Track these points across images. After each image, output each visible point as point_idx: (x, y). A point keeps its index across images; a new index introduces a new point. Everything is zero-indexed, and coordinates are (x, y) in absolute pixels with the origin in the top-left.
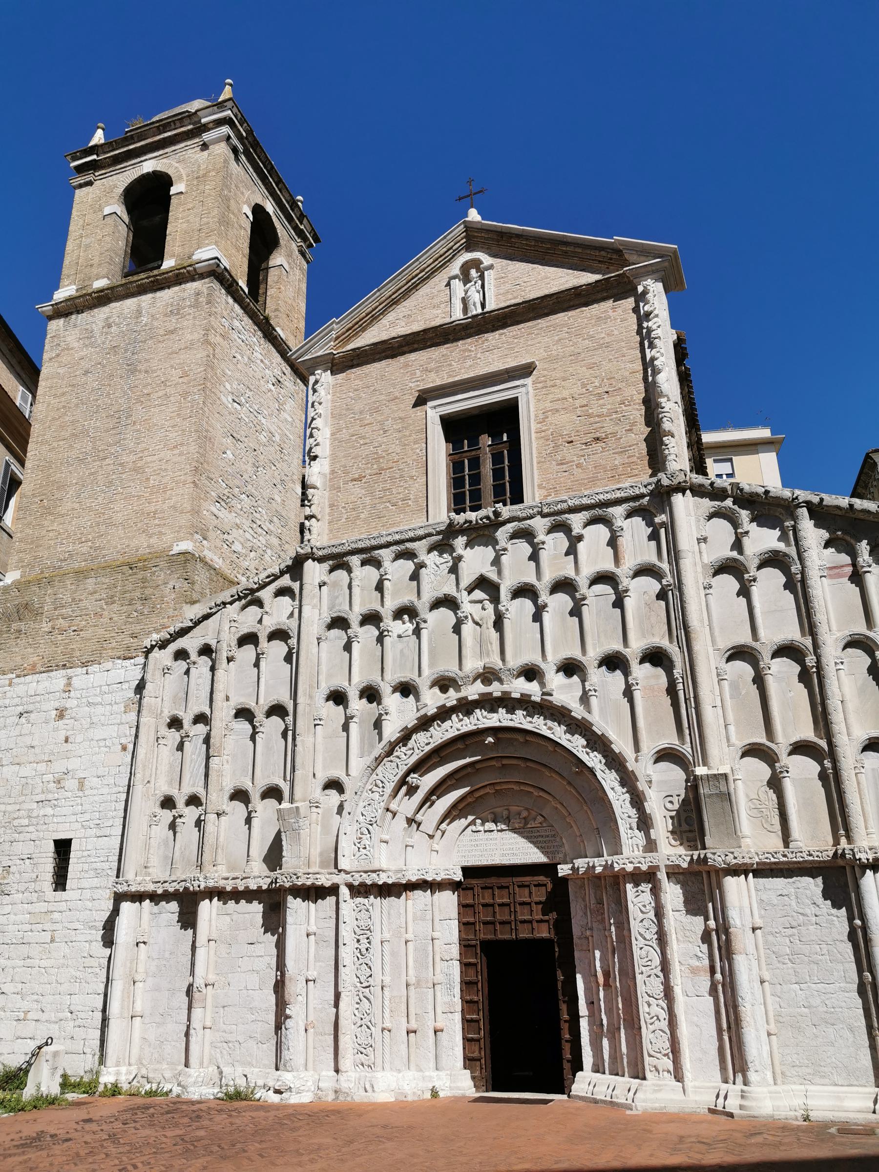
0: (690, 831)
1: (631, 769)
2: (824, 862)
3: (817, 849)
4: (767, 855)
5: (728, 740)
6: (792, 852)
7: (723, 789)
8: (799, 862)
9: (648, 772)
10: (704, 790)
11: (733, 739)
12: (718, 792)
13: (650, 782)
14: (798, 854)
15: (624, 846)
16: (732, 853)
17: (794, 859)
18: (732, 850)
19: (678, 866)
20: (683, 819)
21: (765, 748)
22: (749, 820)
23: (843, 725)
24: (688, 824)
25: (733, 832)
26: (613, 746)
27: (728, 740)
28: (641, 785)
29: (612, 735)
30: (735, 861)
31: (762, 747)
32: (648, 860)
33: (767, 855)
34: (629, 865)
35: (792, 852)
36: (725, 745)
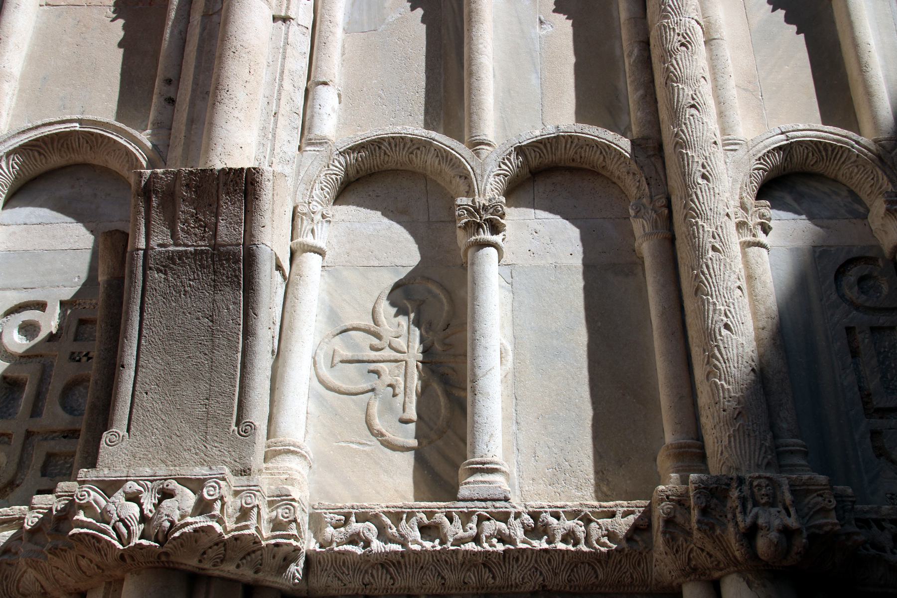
2: (596, 557)
3: (572, 504)
4: (355, 526)
6: (466, 517)
7: (228, 232)
10: (151, 239)
12: (203, 246)
16: (196, 485)
17: (471, 546)
18: (200, 471)
20: (56, 386)
21: (431, 160)
22: (320, 400)
23: (706, 90)
25: (227, 401)
27: (305, 128)
30: (201, 521)
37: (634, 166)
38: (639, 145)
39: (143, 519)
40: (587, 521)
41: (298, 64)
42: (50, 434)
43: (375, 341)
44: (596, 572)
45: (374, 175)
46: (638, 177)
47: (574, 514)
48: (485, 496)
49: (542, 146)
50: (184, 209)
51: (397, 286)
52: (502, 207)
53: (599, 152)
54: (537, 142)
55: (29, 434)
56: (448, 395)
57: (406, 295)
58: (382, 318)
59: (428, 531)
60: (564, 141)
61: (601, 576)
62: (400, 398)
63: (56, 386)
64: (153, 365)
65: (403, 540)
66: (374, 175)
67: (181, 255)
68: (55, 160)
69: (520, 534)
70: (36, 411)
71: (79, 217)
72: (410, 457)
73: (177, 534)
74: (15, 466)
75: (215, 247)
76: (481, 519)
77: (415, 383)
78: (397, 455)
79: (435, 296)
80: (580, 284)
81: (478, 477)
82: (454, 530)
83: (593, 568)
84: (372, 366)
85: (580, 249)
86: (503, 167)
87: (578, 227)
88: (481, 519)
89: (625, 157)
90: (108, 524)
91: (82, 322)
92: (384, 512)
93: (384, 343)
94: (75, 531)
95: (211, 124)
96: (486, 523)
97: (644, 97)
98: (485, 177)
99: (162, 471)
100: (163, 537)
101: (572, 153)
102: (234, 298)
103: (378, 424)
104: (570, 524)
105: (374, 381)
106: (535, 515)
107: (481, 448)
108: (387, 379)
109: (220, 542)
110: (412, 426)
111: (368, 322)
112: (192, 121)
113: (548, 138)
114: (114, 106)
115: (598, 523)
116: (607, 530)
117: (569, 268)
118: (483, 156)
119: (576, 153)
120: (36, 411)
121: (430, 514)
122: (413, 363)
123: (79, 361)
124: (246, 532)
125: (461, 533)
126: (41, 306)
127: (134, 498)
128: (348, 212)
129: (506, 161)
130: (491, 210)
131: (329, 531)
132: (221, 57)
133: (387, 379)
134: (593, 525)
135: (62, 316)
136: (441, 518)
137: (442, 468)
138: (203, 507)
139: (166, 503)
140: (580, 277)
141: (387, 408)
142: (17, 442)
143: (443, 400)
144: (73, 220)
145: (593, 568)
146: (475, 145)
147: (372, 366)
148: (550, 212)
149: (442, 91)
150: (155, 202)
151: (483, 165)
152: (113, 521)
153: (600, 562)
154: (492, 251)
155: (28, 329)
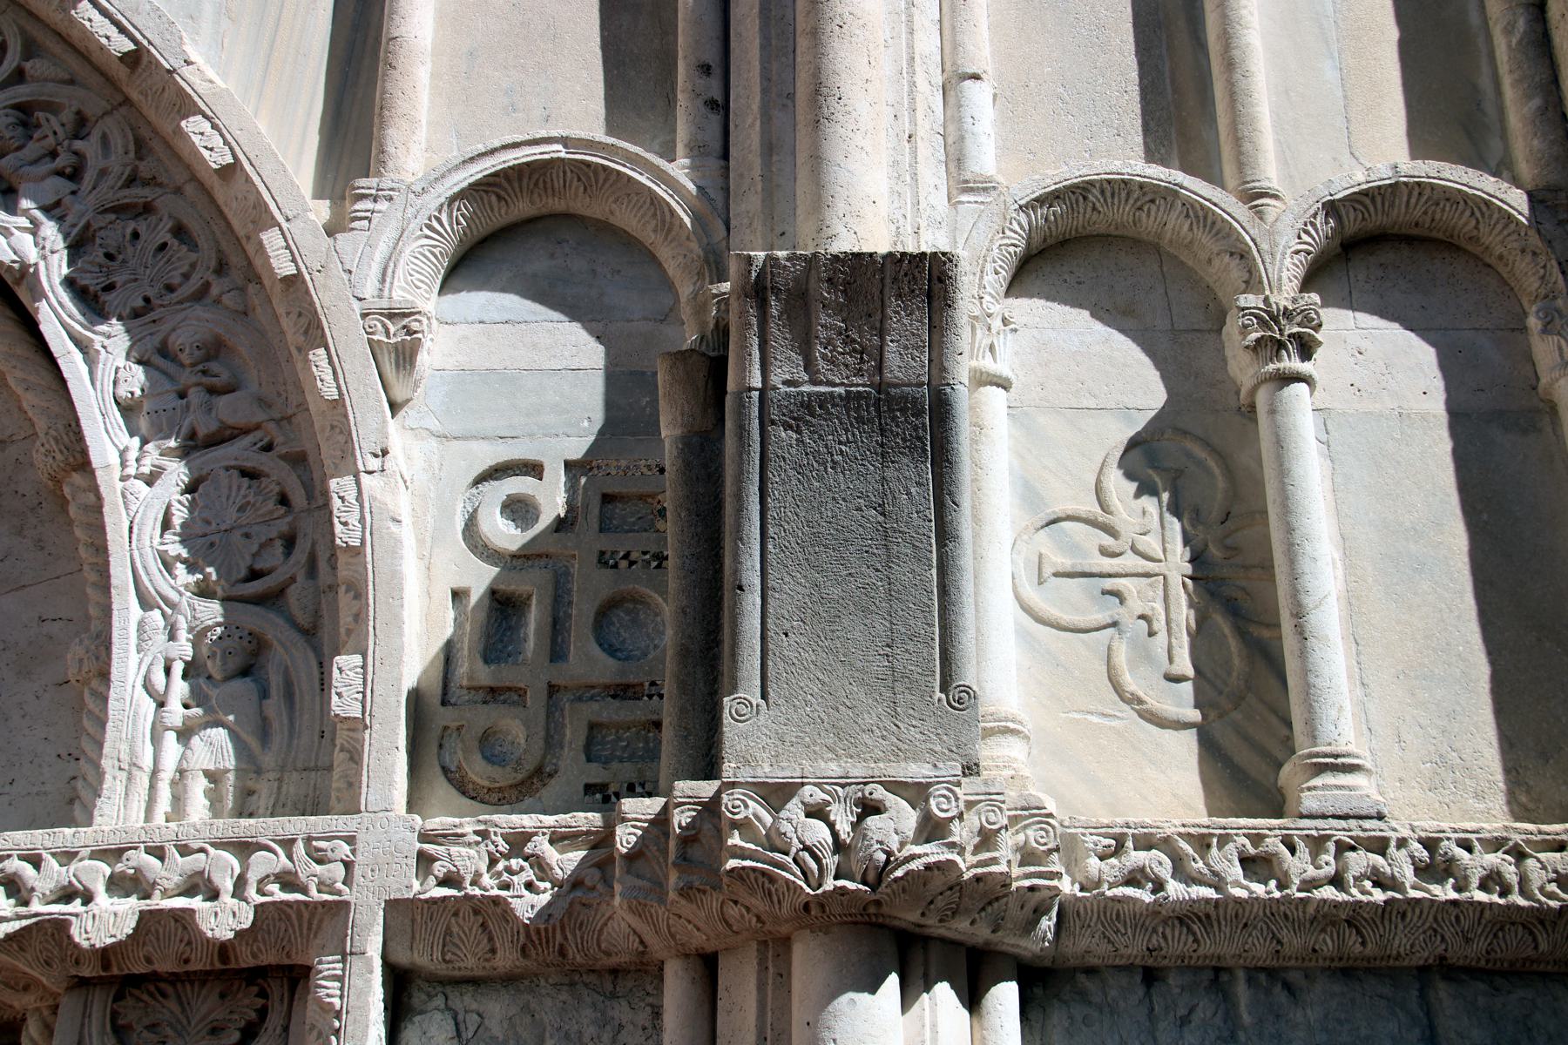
0: (623, 692)
1: (283, 266)
2: (1540, 917)
4: (1136, 858)
5: (956, 157)
6: (1317, 844)
8: (1355, 916)
9: (400, 295)
10: (767, 370)
11: (985, 159)
12: (860, 385)
13: (406, 356)
14: (1359, 861)
15: (113, 784)
16: (916, 793)
17: (1328, 892)
18: (916, 771)
19: (493, 911)
20: (582, 612)
21: (1175, 225)
24: (612, 651)
26: (193, 126)
27: (956, 157)
28: (343, 370)
29: (205, 61)
30: (933, 853)
31: (1148, 224)
32: (262, 863)
33: (1136, 858)
34: (103, 900)
35: (1317, 844)
36: (933, 177)
37: (1534, 240)
38: (1542, 202)
39: (839, 846)
40: (1519, 855)
41: (928, 43)
42: (586, 692)
43: (1108, 541)
44: (1535, 940)
45: (1077, 246)
46: (1542, 259)
47: (1495, 844)
48: (1346, 811)
49: (1368, 201)
50: (826, 322)
51: (1133, 444)
52: (1317, 313)
53: (1468, 213)
54: (1360, 193)
55: (553, 689)
56: (1242, 634)
57: (1150, 458)
58: (1114, 501)
59: (1256, 865)
60: (1405, 191)
61: (1543, 946)
62: (1162, 637)
63: (582, 612)
64: (791, 589)
65: (1218, 882)
66: (1077, 246)
67: (823, 400)
68: (523, 208)
69: (1408, 874)
70: (557, 653)
71: (573, 311)
72: (1189, 739)
73: (899, 873)
74: (541, 743)
75: (880, 387)
76: (1342, 848)
77: (1184, 614)
78: (1168, 734)
79: (1200, 463)
80: (1446, 445)
81: (1328, 779)
82: (1299, 865)
83: (1531, 933)
84: (1109, 584)
85: (1439, 384)
86: (1305, 238)
87: (1432, 344)
88: (1342, 848)
89: (1518, 223)
90: (787, 854)
91: (607, 499)
92: (1180, 835)
93: (1121, 545)
94: (732, 863)
95: (817, 160)
96: (1350, 855)
97: (1543, 111)
98: (1278, 257)
99: (858, 771)
100: (877, 876)
101: (1418, 213)
102: (912, 477)
103: (1131, 683)
104: (1493, 859)
105: (1111, 610)
106: (1430, 844)
107: (1326, 730)
108: (1136, 605)
109: (958, 886)
110: (1187, 688)
111: (1090, 507)
112: (769, 148)
113: (1379, 187)
114: (598, 106)
115: (1539, 860)
116: (1556, 871)
117: (1424, 417)
118: (1270, 218)
119: (1425, 213)
120: (557, 653)
121: (1257, 839)
122: (1176, 581)
123: (615, 566)
124: (994, 869)
125: (1311, 872)
126: (534, 469)
127: (817, 812)
128: (1032, 310)
129: (1309, 228)
130: (1299, 318)
131: (1094, 863)
132: (815, 34)
133: (1136, 605)
134: (1530, 862)
135: (571, 488)
136: (1274, 844)
137: (1244, 757)
138: (932, 829)
139: (872, 821)
140: (1445, 433)
141: (1143, 656)
142: (536, 700)
143: (1233, 644)
144: (562, 317)
145: (1531, 933)
146: (1253, 197)
147: (1109, 584)
148: (1382, 316)
149: (1169, 88)
150: (775, 308)
151: (1271, 233)
152: (794, 850)
153: (1542, 922)
154: (1302, 387)
155: (519, 509)
